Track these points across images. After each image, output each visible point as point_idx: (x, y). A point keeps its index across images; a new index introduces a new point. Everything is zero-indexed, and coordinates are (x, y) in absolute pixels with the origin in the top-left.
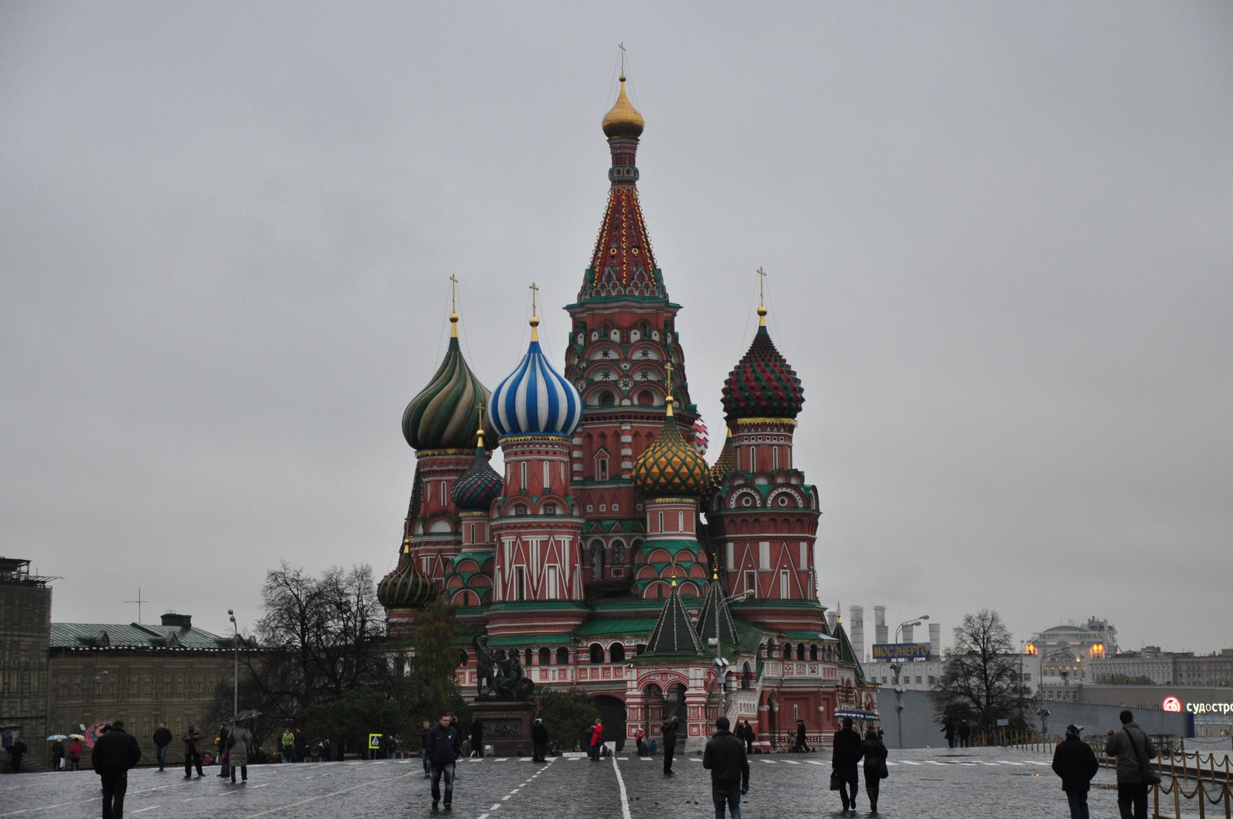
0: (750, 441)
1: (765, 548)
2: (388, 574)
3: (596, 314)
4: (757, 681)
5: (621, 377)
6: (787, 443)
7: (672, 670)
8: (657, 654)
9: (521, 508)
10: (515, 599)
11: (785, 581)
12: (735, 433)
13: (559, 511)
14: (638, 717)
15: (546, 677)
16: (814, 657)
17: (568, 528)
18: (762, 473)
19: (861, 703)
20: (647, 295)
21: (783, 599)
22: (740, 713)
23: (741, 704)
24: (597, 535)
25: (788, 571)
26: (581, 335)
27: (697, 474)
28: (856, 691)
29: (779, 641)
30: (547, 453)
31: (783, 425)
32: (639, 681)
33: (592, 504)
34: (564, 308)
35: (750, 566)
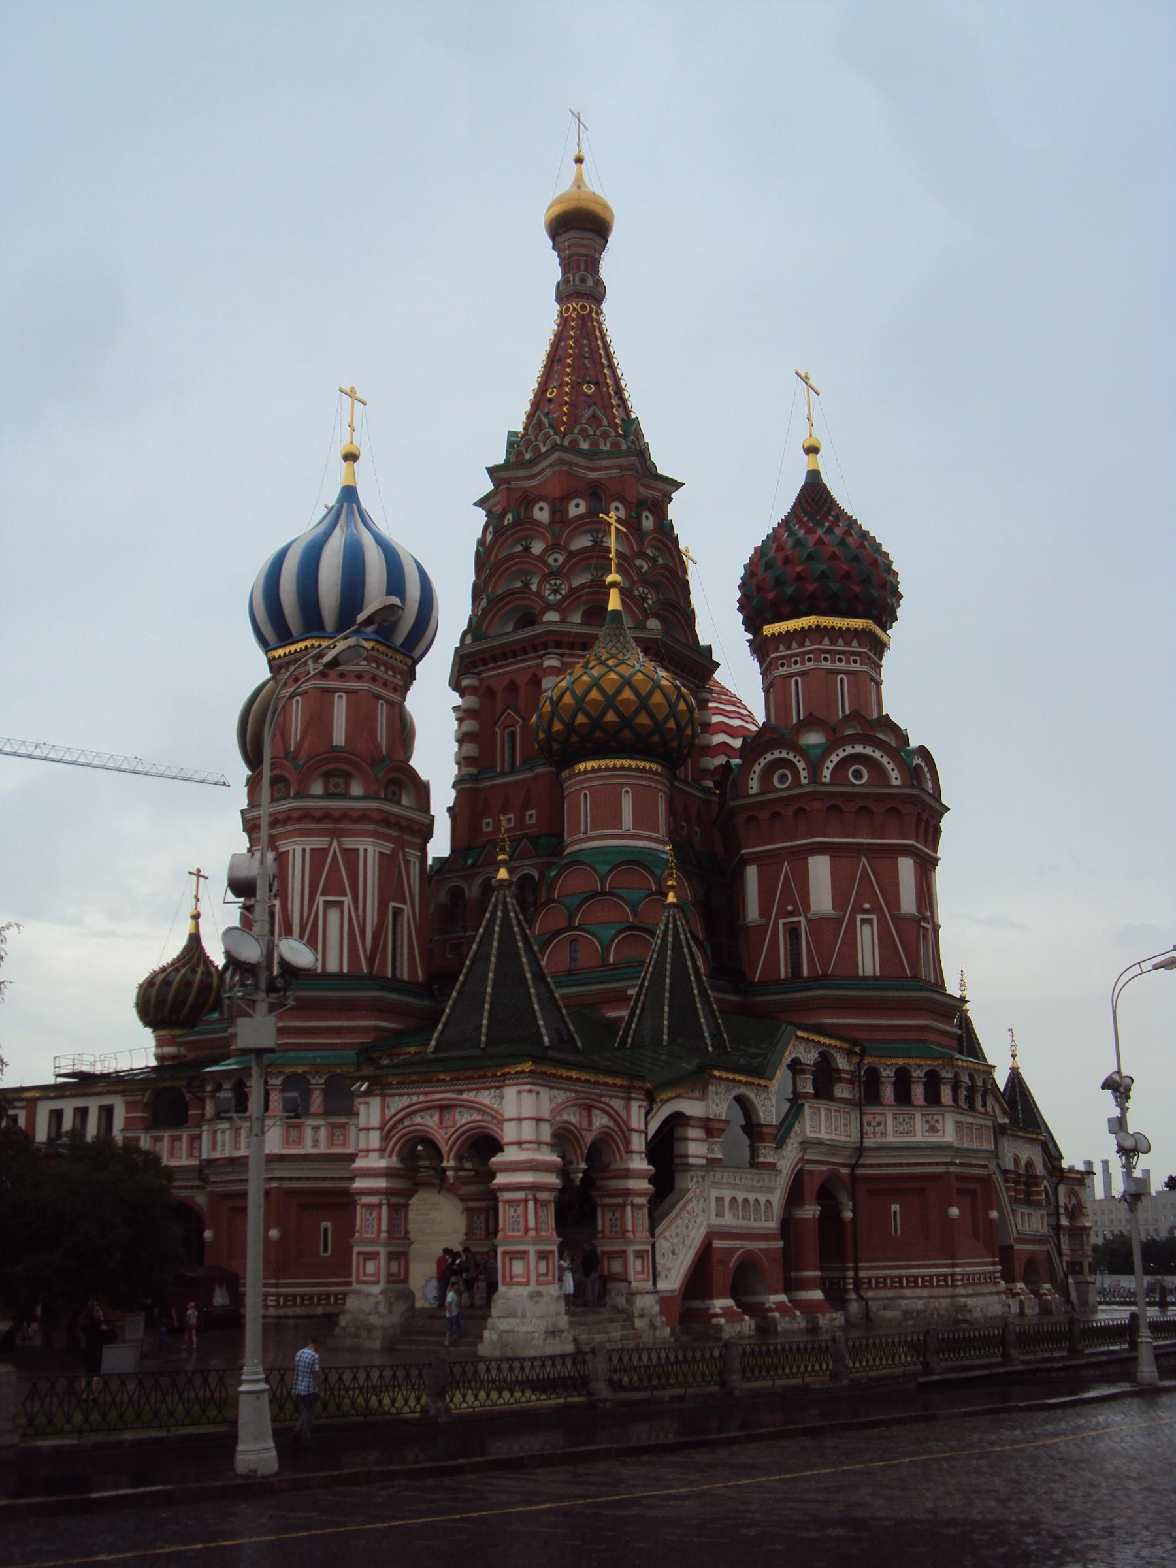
0: (789, 666)
1: (820, 869)
2: (157, 969)
3: (515, 489)
4: (779, 1146)
5: (545, 578)
6: (865, 668)
7: (465, 1096)
8: (439, 1055)
11: (867, 939)
13: (356, 789)
15: (299, 1142)
16: (933, 1098)
17: (371, 820)
18: (811, 722)
19: (1057, 1206)
20: (605, 449)
21: (864, 977)
22: (714, 1221)
23: (720, 1200)
25: (874, 917)
26: (491, 529)
27: (661, 704)
28: (1045, 1183)
29: (849, 1062)
32: (387, 1130)
34: (476, 504)
35: (790, 908)
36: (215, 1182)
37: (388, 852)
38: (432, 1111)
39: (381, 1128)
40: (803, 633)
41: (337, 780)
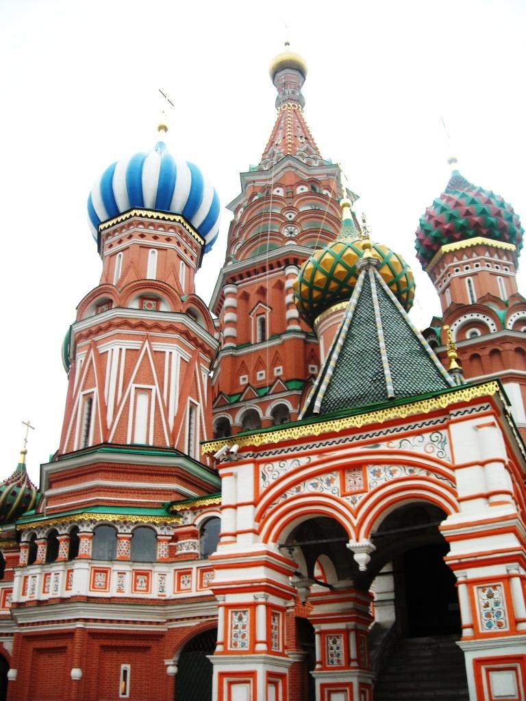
0: (462, 270)
7: (383, 447)
9: (104, 307)
10: (75, 450)
12: (439, 273)
13: (163, 308)
14: (254, 642)
15: (106, 586)
20: (317, 165)
24: (247, 404)
26: (242, 210)
27: (397, 263)
30: (155, 238)
31: (507, 252)
32: (263, 505)
33: (247, 373)
36: (23, 625)
37: (188, 361)
38: (329, 476)
39: (255, 504)
40: (473, 248)
41: (151, 302)
